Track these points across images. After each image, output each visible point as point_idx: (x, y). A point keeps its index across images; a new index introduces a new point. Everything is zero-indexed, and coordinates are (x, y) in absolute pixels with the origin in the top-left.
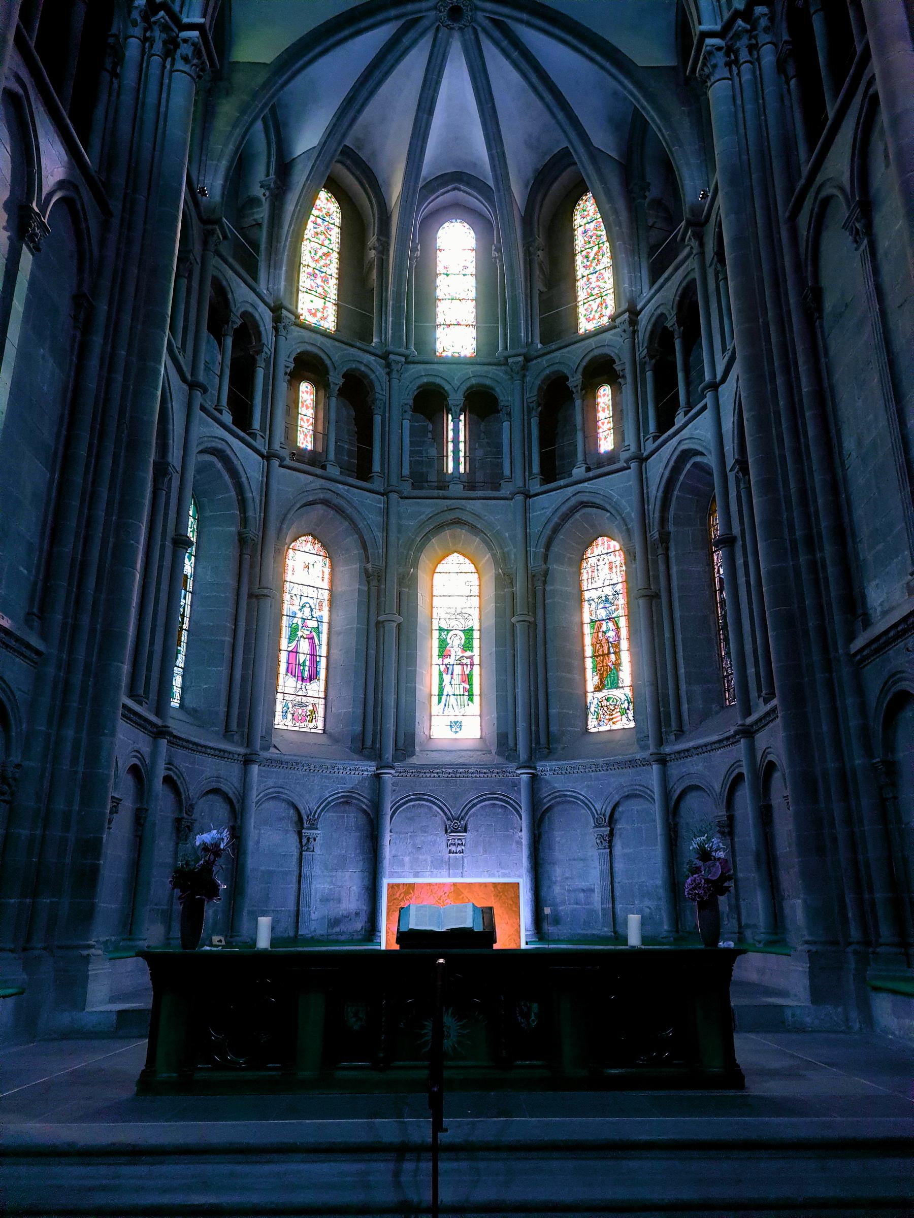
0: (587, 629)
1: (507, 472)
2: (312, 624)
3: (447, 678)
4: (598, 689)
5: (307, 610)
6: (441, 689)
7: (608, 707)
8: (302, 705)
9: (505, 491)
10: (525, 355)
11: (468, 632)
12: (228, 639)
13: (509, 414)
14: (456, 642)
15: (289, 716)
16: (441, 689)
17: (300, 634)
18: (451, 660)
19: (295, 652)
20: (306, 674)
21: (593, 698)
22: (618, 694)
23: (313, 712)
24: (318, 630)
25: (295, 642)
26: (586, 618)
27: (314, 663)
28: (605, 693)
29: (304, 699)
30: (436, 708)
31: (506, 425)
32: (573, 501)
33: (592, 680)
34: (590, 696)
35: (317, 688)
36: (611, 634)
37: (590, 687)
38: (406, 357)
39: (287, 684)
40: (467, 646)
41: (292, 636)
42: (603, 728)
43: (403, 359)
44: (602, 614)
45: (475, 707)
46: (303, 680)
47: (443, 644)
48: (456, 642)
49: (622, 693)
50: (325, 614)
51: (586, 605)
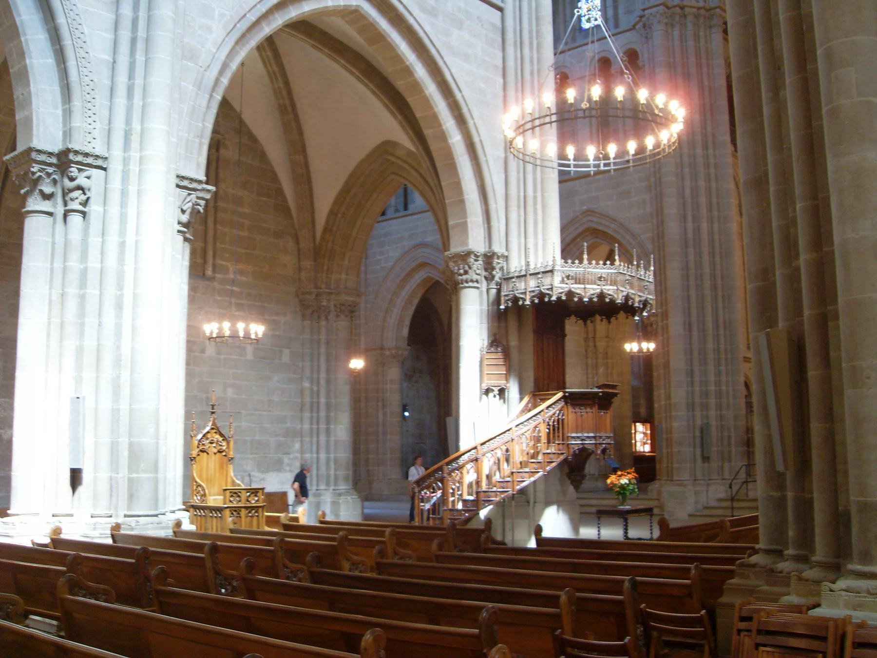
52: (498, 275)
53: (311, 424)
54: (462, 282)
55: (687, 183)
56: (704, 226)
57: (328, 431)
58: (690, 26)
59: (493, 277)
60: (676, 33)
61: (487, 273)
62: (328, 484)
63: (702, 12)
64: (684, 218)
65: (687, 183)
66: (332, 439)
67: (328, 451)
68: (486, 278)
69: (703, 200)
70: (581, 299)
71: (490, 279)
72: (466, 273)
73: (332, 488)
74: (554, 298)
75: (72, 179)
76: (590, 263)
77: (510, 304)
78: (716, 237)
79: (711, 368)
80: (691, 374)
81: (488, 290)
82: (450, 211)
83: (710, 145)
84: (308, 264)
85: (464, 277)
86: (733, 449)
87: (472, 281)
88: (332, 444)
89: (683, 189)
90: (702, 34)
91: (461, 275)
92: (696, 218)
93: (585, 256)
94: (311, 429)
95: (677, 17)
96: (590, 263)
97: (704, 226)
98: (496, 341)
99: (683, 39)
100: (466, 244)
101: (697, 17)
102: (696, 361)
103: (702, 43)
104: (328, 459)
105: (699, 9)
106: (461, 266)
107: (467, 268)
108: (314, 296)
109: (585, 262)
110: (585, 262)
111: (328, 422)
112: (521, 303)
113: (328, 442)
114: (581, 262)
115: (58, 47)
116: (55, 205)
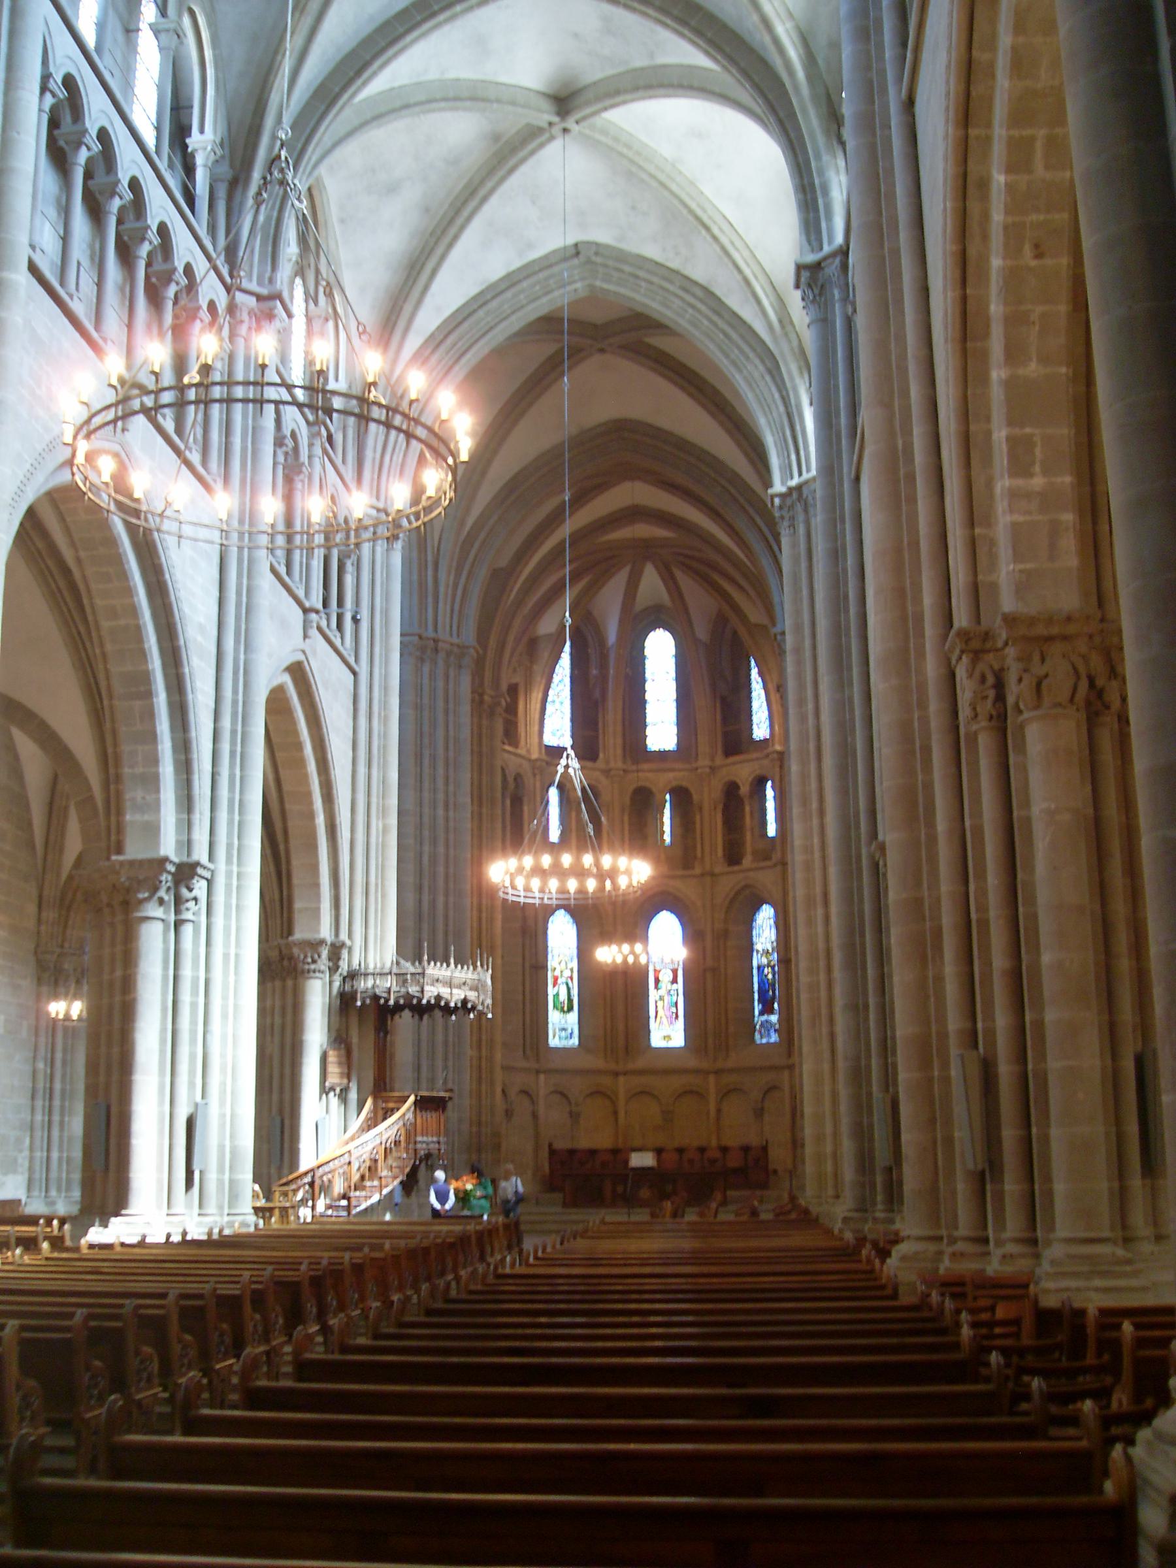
0: (755, 972)
1: (699, 854)
2: (567, 973)
3: (660, 1004)
4: (761, 1013)
5: (563, 964)
6: (657, 1012)
7: (766, 1025)
8: (564, 1029)
9: (697, 871)
10: (711, 767)
11: (675, 972)
12: (520, 997)
13: (701, 809)
14: (665, 977)
15: (557, 1037)
16: (657, 1012)
17: (559, 981)
18: (662, 992)
19: (557, 995)
20: (566, 1009)
21: (759, 1019)
22: (774, 1018)
23: (571, 1034)
24: (571, 978)
25: (556, 988)
26: (755, 964)
27: (570, 1000)
28: (764, 1018)
29: (565, 1026)
30: (653, 1025)
31: (698, 817)
32: (743, 883)
33: (757, 1008)
34: (756, 1019)
35: (573, 1018)
36: (770, 976)
37: (757, 1012)
38: (624, 771)
39: (554, 1017)
40: (675, 981)
41: (555, 984)
42: (764, 1041)
43: (622, 772)
44: (765, 961)
45: (680, 1023)
46: (564, 1012)
47: (657, 981)
48: (665, 977)
49: (774, 1018)
50: (574, 964)
51: (755, 954)
52: (344, 967)
53: (44, 1115)
54: (309, 971)
55: (426, 848)
56: (441, 900)
57: (62, 1123)
58: (441, 663)
59: (338, 967)
60: (426, 669)
61: (331, 964)
62: (59, 1190)
63: (456, 650)
64: (420, 888)
65: (426, 848)
66: (66, 1134)
67: (61, 1150)
68: (329, 968)
69: (441, 869)
70: (447, 1004)
71: (334, 969)
72: (314, 961)
73: (63, 1194)
74: (424, 1002)
75: (191, 890)
76: (456, 967)
77: (368, 1001)
78: (451, 913)
79: (439, 1063)
80: (418, 1069)
81: (331, 983)
82: (297, 893)
83: (451, 806)
84: (50, 915)
85: (313, 967)
86: (456, 1156)
87: (319, 971)
88: (66, 1139)
89: (421, 854)
90: (452, 673)
91: (308, 964)
92: (433, 890)
93: (452, 961)
94: (43, 1121)
95: (429, 651)
96: (456, 967)
97: (441, 900)
98: (339, 1038)
99: (432, 676)
100: (318, 931)
101: (449, 654)
102: (424, 1054)
103: (451, 686)
104: (60, 1159)
105: (452, 644)
106: (309, 955)
107: (316, 956)
108: (55, 956)
109: (452, 965)
110: (452, 965)
111: (62, 1115)
112: (382, 1001)
113: (61, 1138)
114: (448, 965)
115: (183, 757)
116: (166, 912)
